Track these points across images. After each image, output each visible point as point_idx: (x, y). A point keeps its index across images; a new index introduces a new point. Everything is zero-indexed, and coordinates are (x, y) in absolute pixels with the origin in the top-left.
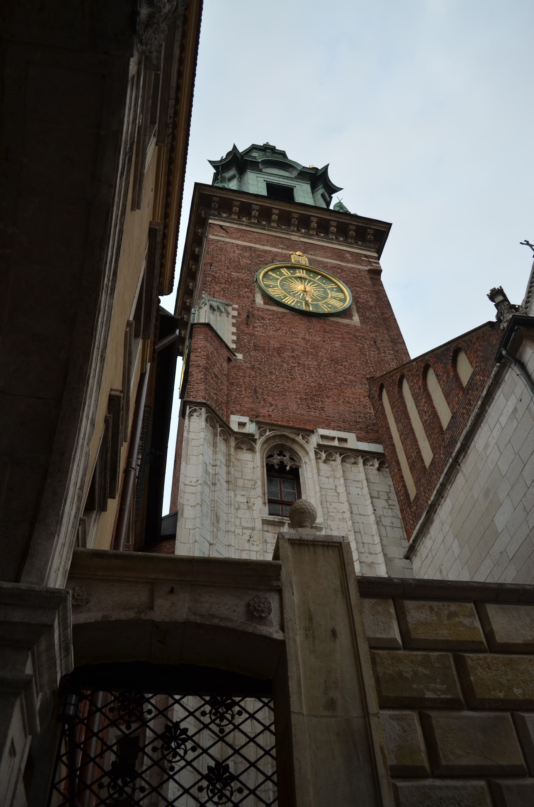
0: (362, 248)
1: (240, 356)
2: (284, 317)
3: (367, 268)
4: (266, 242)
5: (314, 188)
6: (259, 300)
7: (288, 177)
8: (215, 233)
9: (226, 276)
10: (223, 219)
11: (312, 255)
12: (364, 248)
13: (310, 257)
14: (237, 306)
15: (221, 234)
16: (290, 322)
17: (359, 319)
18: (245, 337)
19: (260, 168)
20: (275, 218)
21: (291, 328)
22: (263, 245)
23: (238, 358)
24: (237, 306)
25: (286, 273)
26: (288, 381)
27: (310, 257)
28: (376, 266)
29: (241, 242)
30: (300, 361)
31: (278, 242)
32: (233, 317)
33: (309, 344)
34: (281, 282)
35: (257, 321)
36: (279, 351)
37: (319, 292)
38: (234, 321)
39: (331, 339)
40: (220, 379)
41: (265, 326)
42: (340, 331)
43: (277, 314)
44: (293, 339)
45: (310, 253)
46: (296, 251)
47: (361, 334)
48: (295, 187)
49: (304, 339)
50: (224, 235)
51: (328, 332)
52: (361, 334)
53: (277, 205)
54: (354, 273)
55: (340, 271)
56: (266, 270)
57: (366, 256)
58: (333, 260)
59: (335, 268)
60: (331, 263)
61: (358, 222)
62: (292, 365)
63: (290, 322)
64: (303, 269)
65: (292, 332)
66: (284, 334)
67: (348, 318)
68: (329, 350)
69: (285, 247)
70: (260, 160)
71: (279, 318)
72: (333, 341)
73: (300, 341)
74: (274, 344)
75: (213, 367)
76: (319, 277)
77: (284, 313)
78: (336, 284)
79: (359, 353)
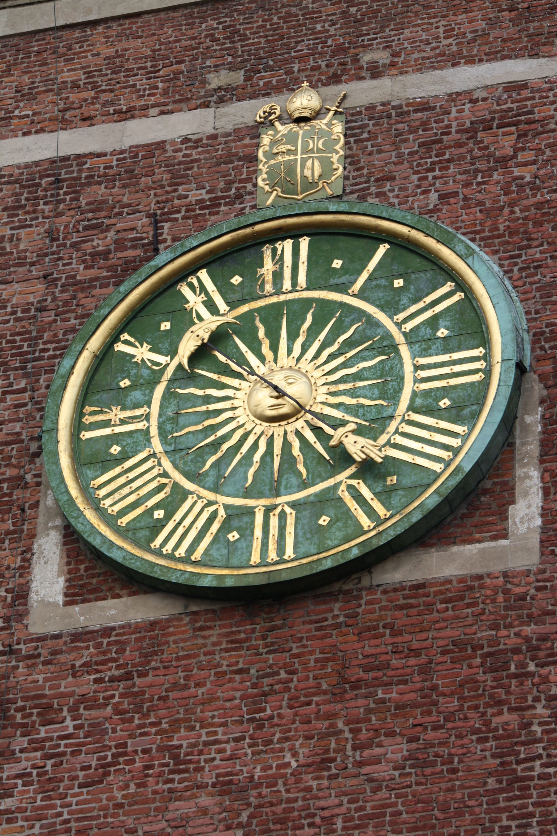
2: (147, 657)
4: (141, 82)
16: (175, 686)
17: (545, 513)
21: (175, 725)
29: (20, 142)
31: (205, 55)
33: (244, 817)
34: (168, 395)
37: (352, 393)
39: (364, 735)
41: (50, 763)
42: (416, 653)
43: (121, 647)
45: (366, 58)
47: (529, 630)
51: (356, 685)
52: (529, 630)
63: (175, 686)
66: (132, 789)
67: (481, 526)
68: (339, 824)
69: (238, 77)
71: (128, 676)
72: (369, 745)
73: (204, 812)
76: (383, 249)
77: (153, 625)
79: (492, 782)
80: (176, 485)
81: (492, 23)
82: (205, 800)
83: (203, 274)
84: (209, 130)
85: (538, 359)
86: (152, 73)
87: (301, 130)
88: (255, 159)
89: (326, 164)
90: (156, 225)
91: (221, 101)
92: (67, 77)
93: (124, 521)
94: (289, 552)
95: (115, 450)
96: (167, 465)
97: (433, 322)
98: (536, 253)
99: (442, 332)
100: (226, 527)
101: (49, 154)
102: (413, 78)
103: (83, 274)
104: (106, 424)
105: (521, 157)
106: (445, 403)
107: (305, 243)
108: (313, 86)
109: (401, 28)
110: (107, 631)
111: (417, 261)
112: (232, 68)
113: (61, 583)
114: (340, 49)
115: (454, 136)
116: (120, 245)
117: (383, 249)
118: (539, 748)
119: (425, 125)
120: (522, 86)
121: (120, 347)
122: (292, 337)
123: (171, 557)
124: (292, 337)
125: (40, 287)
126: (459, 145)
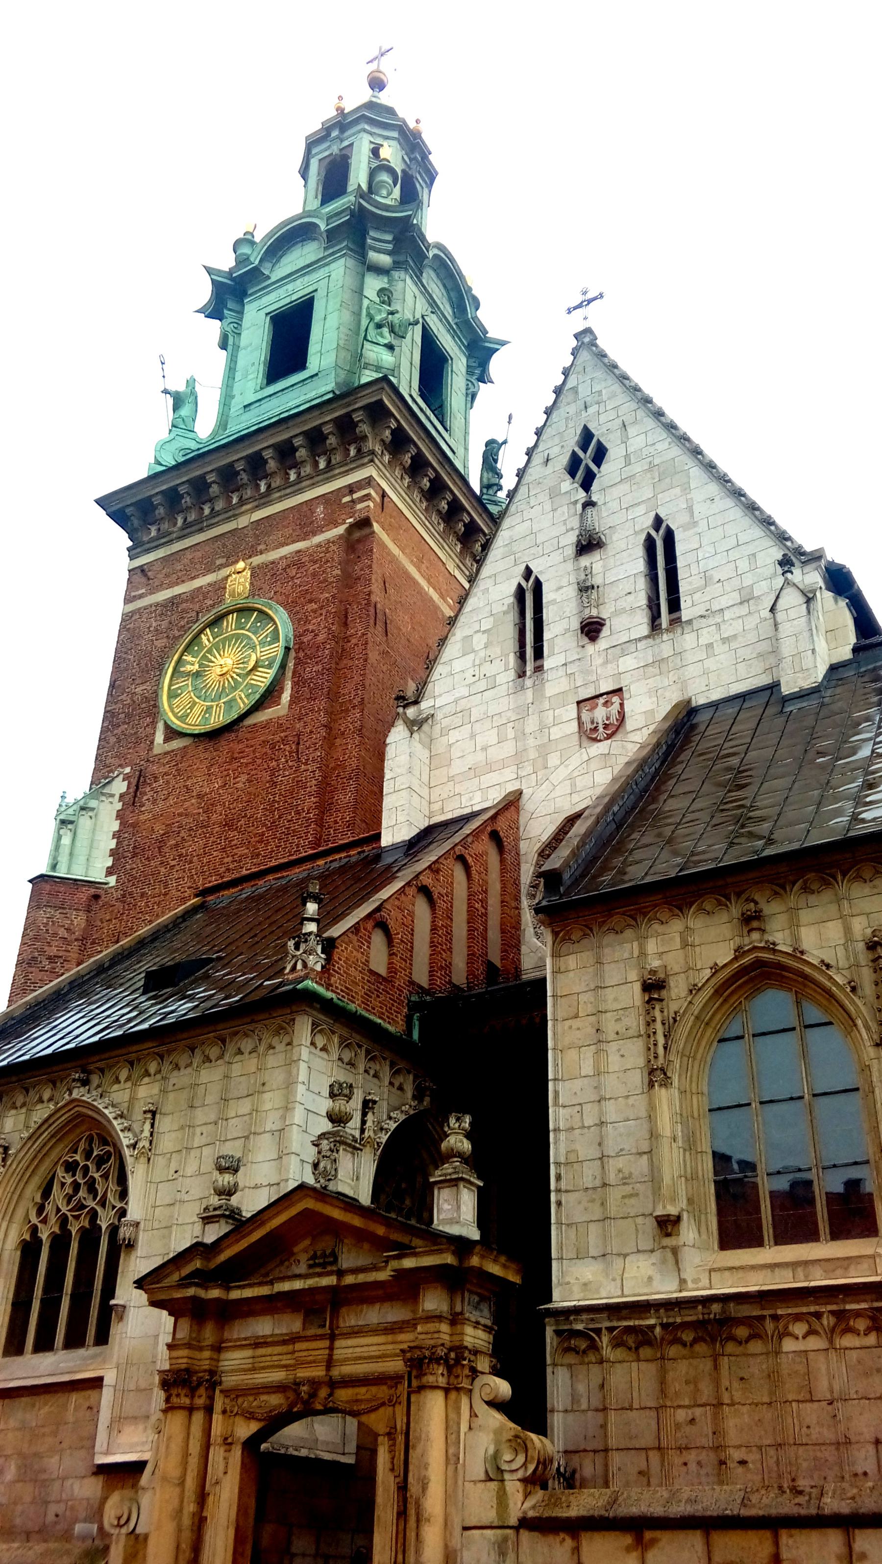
0: (346, 468)
1: (112, 880)
3: (341, 530)
5: (360, 250)
6: (159, 737)
7: (308, 266)
8: (133, 594)
9: (129, 701)
10: (148, 546)
11: (261, 553)
12: (352, 466)
13: (257, 560)
14: (128, 770)
15: (141, 592)
18: (126, 835)
19: (266, 272)
20: (214, 492)
22: (193, 578)
23: (111, 885)
24: (128, 770)
25: (208, 640)
26: (159, 904)
27: (257, 560)
28: (361, 510)
30: (183, 851)
32: (122, 796)
35: (148, 789)
36: (161, 843)
38: (119, 806)
40: (61, 957)
42: (252, 746)
44: (187, 804)
46: (237, 562)
47: (282, 735)
48: (316, 290)
49: (200, 796)
50: (143, 591)
53: (209, 463)
54: (315, 562)
55: (293, 572)
56: (176, 657)
57: (351, 489)
58: (293, 542)
59: (289, 566)
60: (285, 557)
61: (334, 410)
62: (173, 863)
64: (232, 612)
65: (186, 786)
69: (225, 560)
70: (257, 262)
73: (193, 805)
74: (160, 829)
75: (46, 948)
76: (255, 614)
77: (185, 747)
78: (275, 623)
80: (194, 701)
81: (293, 530)
82: (193, 801)
83: (208, 630)
84: (215, 580)
85: (294, 644)
86: (201, 563)
87: (238, 576)
88: (225, 588)
89: (245, 588)
90: (198, 613)
91: (219, 569)
92: (179, 568)
93: (179, 714)
94: (221, 718)
95: (179, 691)
96: (192, 694)
97: (266, 637)
98: (298, 608)
99: (269, 639)
100: (205, 714)
101: (171, 595)
102: (272, 553)
103: (177, 633)
104: (178, 683)
105: (298, 576)
106: (267, 663)
107: (235, 615)
108: (243, 560)
109: (269, 536)
110: (173, 751)
111: (265, 617)
112: (223, 557)
113: (162, 737)
114: (252, 546)
115: (280, 571)
116: (188, 623)
117: (255, 614)
118: (281, 772)
119: (272, 569)
120: (299, 551)
121: (184, 657)
122: (229, 646)
123: (190, 725)
124: (229, 646)
125: (165, 640)
126: (281, 574)
